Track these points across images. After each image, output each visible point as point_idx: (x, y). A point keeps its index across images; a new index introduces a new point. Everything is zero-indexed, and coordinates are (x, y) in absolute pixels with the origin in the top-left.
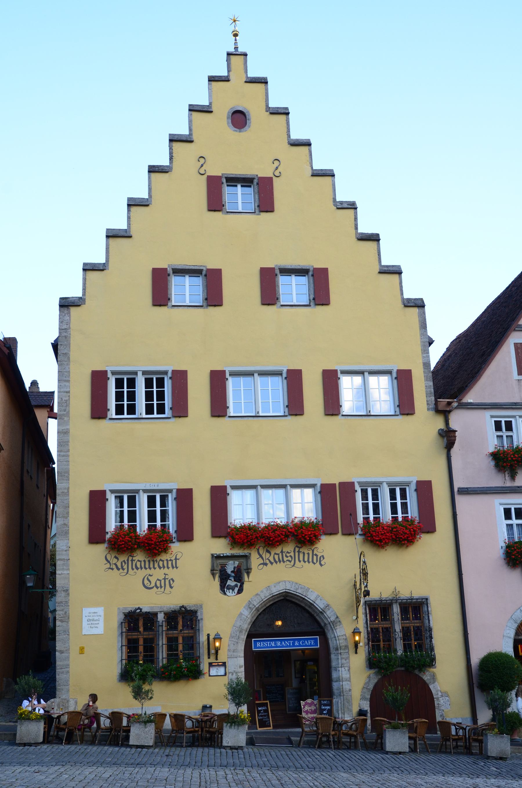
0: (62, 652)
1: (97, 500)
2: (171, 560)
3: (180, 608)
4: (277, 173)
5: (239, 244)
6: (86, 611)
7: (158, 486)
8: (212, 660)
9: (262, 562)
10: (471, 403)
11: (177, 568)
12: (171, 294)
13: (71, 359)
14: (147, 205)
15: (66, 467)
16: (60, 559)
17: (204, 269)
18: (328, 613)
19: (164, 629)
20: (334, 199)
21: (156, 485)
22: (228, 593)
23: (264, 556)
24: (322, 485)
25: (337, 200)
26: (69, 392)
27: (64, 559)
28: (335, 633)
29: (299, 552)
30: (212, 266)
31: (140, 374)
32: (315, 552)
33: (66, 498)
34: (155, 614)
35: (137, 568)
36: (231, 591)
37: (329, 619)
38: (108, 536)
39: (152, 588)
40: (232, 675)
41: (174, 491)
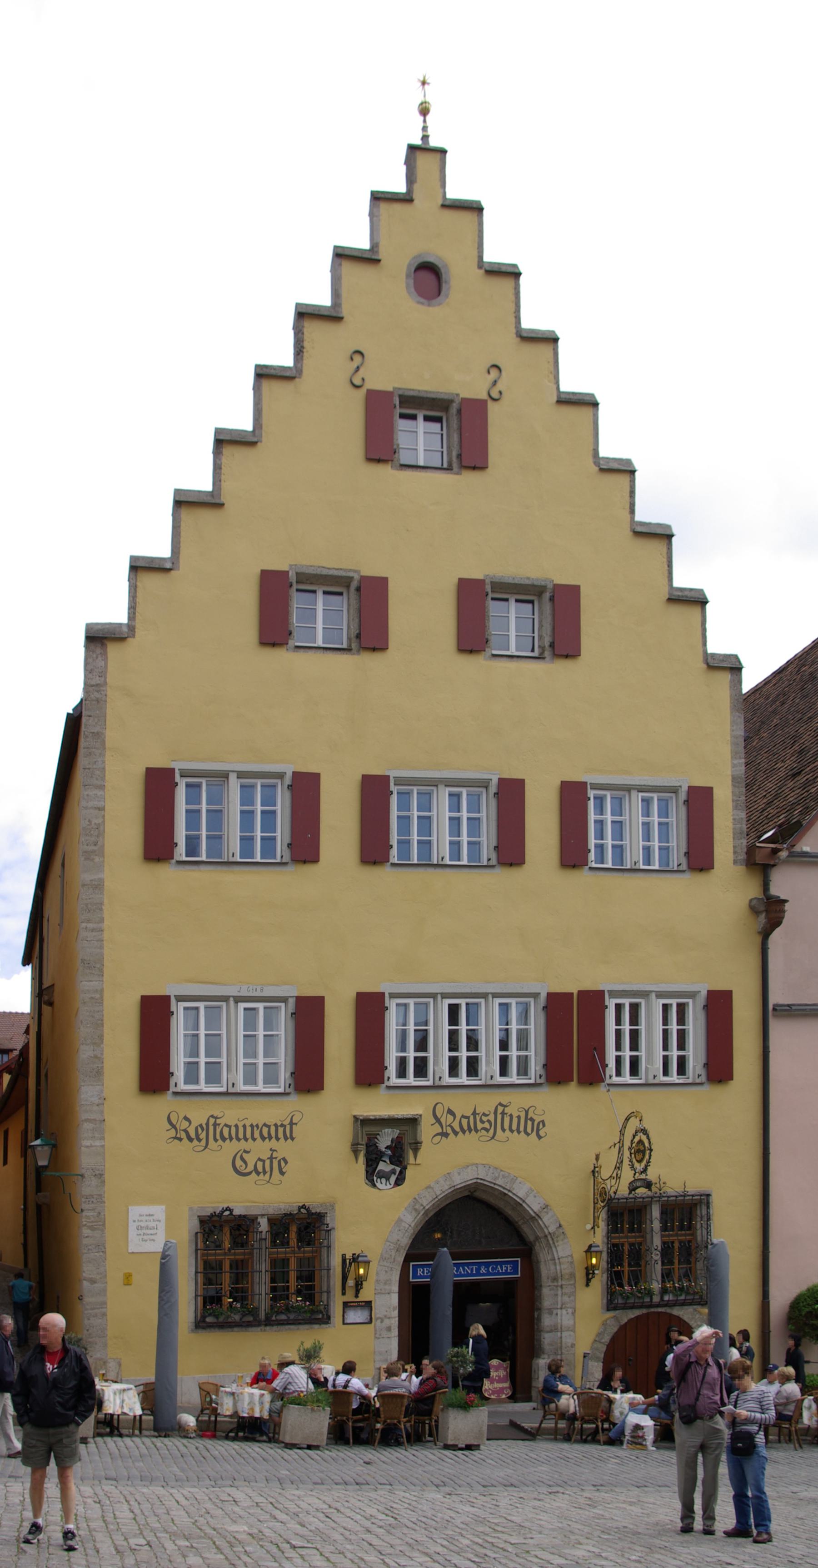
0: (93, 1281)
3: (299, 1210)
4: (495, 395)
6: (136, 1212)
7: (262, 990)
8: (350, 1297)
9: (440, 1131)
10: (807, 853)
11: (293, 1139)
13: (108, 745)
16: (87, 1120)
17: (356, 577)
22: (378, 1185)
23: (443, 1120)
24: (551, 996)
26: (102, 809)
27: (95, 1120)
28: (555, 1254)
30: (368, 571)
32: (530, 1115)
35: (224, 1139)
36: (384, 1180)
37: (546, 1230)
39: (249, 1173)
40: (382, 1322)
41: (292, 1002)
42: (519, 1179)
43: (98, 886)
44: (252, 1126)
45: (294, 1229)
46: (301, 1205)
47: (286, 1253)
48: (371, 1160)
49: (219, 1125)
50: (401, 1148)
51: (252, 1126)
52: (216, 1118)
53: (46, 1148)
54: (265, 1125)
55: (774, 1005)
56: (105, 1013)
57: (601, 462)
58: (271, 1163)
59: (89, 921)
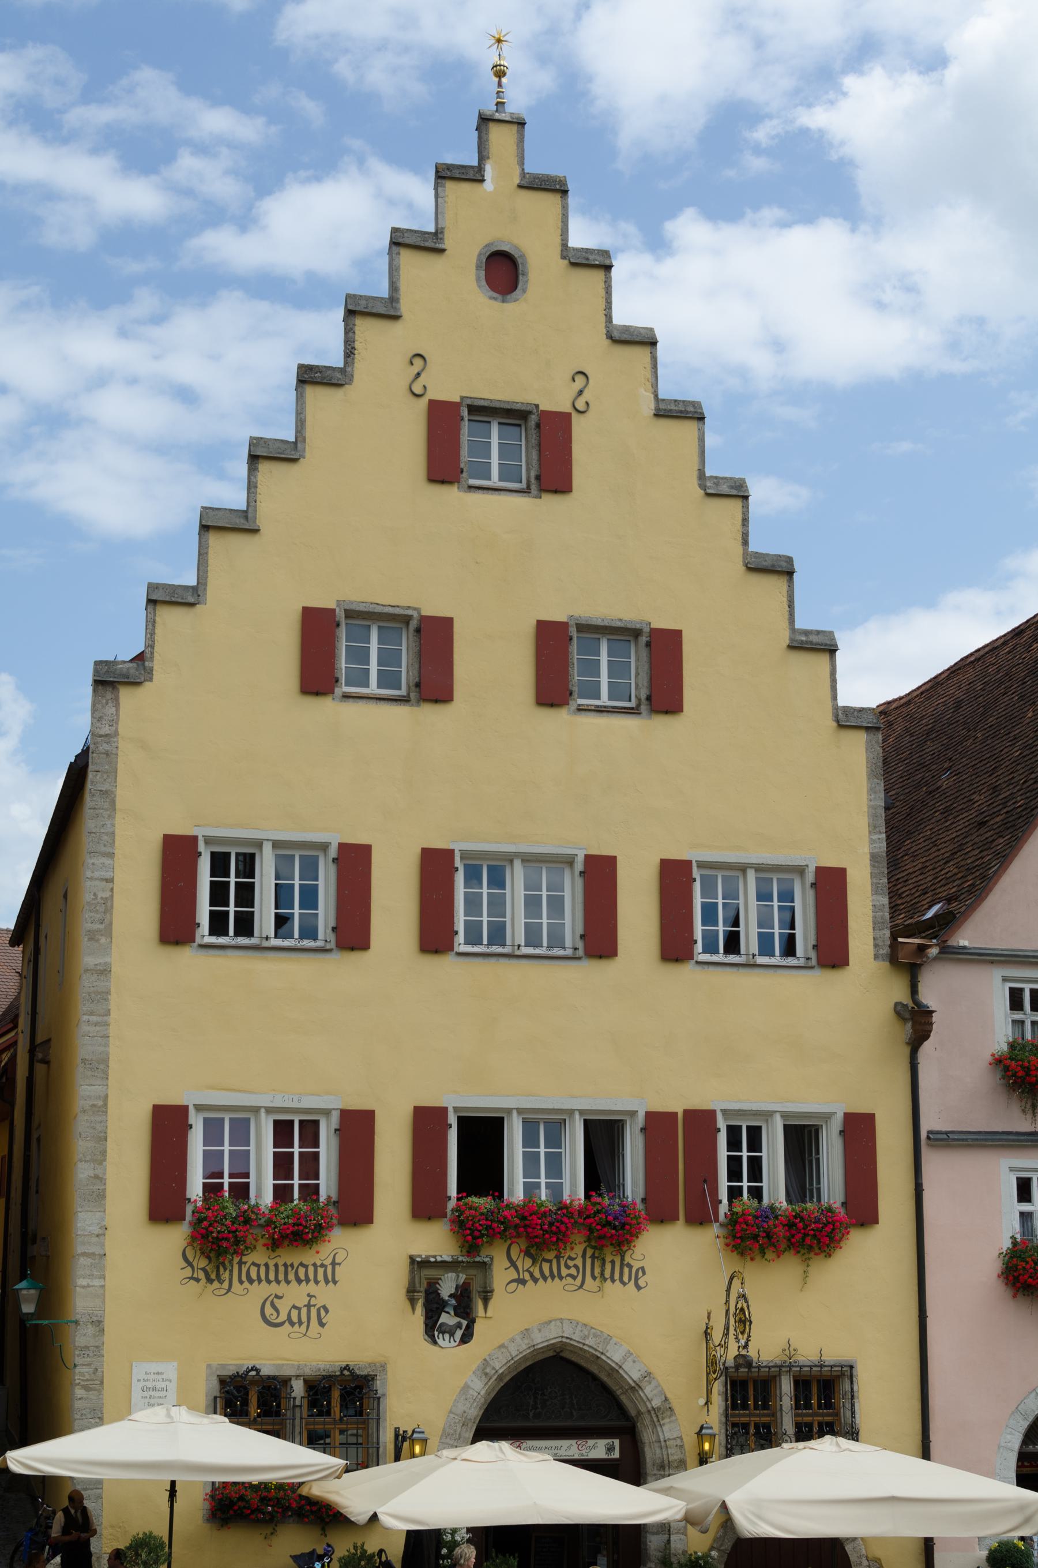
1: (168, 1125)
2: (322, 1265)
4: (580, 405)
5: (496, 566)
7: (299, 1101)
10: (965, 947)
11: (335, 1282)
13: (118, 806)
14: (294, 460)
15: (102, 1049)
16: (84, 1254)
17: (415, 614)
18: (648, 1390)
20: (701, 475)
22: (440, 1341)
23: (519, 1264)
25: (708, 474)
26: (111, 880)
27: (94, 1254)
28: (660, 1434)
29: (593, 1257)
30: (430, 610)
31: (267, 848)
32: (628, 1259)
33: (99, 1119)
35: (251, 1281)
36: (447, 1336)
37: (648, 1403)
38: (189, 1209)
41: (335, 1117)
42: (614, 1339)
43: (104, 971)
45: (336, 1394)
46: (344, 1364)
47: (324, 1423)
48: (431, 1310)
49: (245, 1263)
50: (469, 1297)
51: (285, 1265)
53: (32, 1292)
55: (929, 1132)
56: (109, 1124)
57: (708, 484)
58: (309, 1311)
59: (92, 1014)
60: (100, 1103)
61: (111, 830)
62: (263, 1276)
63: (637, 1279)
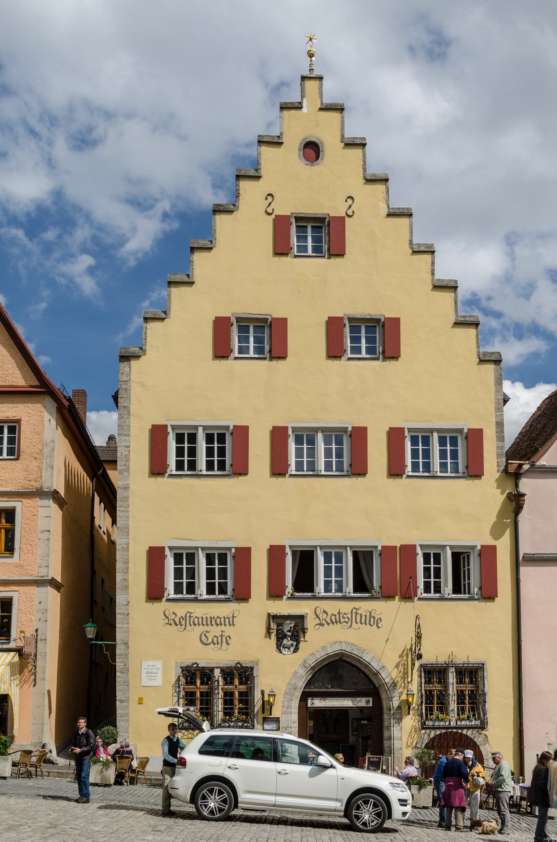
0: (122, 701)
4: (350, 213)
11: (234, 625)
12: (234, 345)
13: (131, 413)
15: (126, 522)
16: (120, 614)
17: (269, 318)
18: (383, 674)
19: (221, 683)
21: (215, 542)
22: (283, 652)
23: (320, 616)
26: (128, 447)
27: (124, 613)
31: (200, 429)
32: (373, 614)
33: (125, 554)
34: (212, 670)
35: (195, 625)
36: (287, 649)
39: (210, 644)
41: (233, 551)
42: (367, 651)
44: (211, 618)
51: (211, 618)
52: (191, 613)
54: (218, 617)
56: (130, 555)
58: (222, 638)
59: (121, 507)
60: (126, 547)
61: (128, 424)
62: (200, 622)
63: (377, 623)
